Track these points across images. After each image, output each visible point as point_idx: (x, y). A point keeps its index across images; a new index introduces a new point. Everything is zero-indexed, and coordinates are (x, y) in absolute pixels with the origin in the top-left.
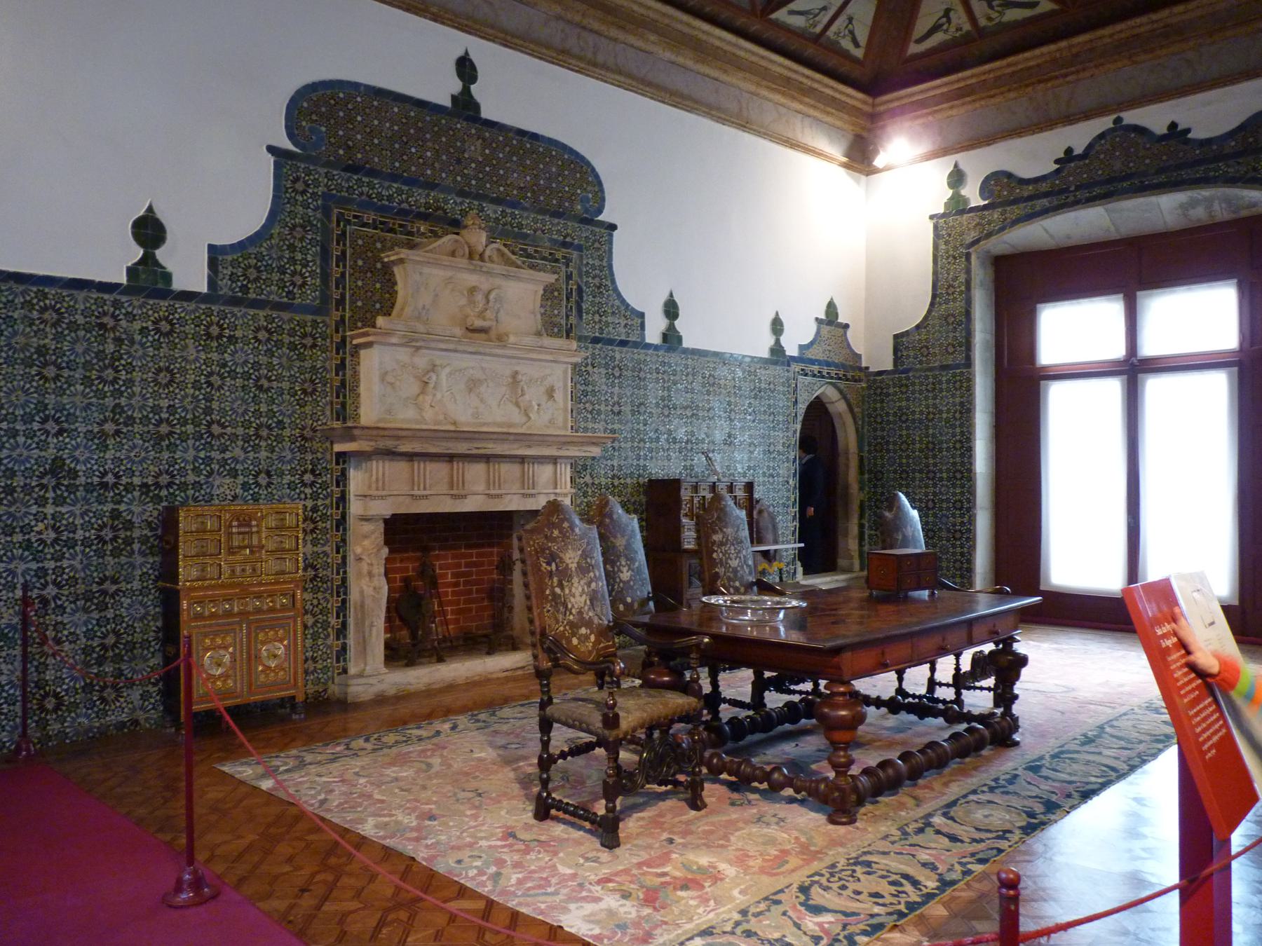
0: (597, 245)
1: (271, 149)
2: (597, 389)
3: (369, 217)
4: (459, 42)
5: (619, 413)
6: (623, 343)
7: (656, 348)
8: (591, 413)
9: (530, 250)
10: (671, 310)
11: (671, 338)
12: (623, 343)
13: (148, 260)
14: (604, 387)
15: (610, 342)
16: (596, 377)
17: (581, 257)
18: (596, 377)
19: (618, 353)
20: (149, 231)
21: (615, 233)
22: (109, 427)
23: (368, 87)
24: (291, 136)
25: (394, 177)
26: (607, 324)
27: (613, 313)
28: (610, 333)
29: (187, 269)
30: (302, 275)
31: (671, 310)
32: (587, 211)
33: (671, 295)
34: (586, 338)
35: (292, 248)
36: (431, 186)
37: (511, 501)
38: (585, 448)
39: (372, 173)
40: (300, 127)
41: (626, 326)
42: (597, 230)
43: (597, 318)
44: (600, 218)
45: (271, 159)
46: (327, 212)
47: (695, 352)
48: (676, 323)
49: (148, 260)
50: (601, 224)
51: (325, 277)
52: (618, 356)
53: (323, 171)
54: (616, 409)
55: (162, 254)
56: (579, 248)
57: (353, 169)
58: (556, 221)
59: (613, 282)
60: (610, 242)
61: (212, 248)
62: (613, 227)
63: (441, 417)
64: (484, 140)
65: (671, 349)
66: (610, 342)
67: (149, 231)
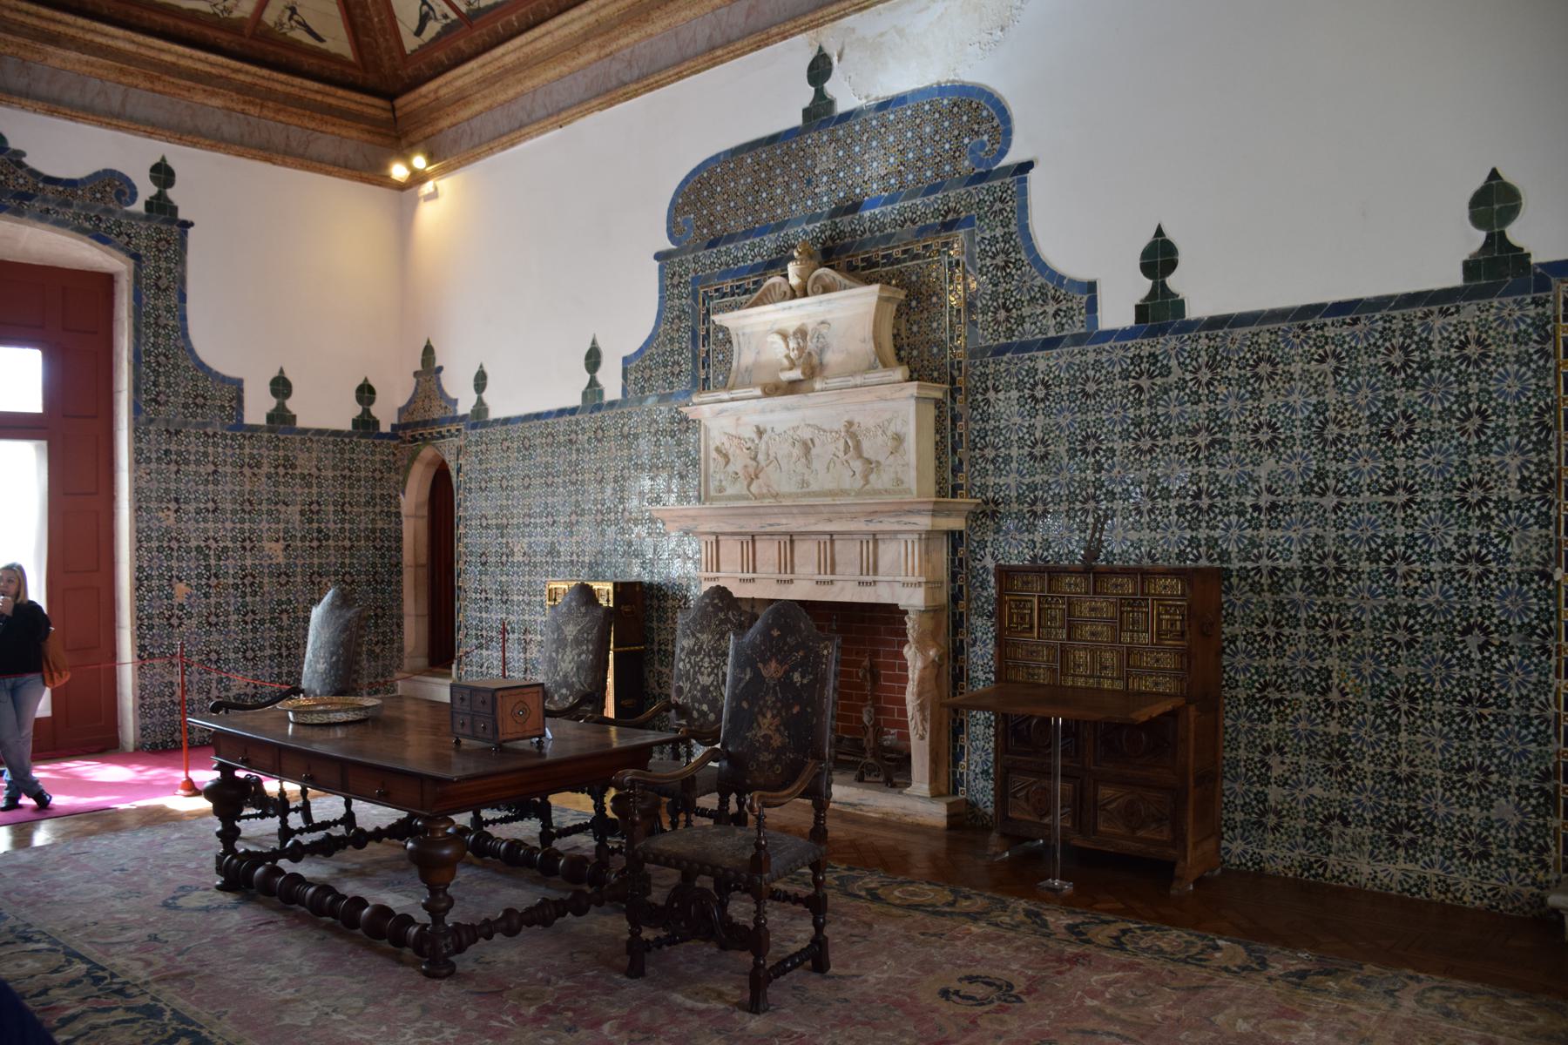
0: (998, 206)
1: (658, 256)
2: (1003, 424)
3: (727, 285)
4: (796, 52)
5: (1045, 457)
6: (1050, 344)
7: (1124, 334)
8: (993, 461)
9: (896, 253)
10: (1160, 258)
11: (1160, 311)
12: (1050, 344)
13: (593, 383)
14: (1018, 420)
15: (1024, 347)
16: (1001, 406)
17: (972, 235)
18: (1001, 406)
19: (1043, 362)
20: (593, 359)
21: (1032, 175)
22: (574, 518)
23: (725, 153)
24: (671, 236)
25: (747, 234)
26: (1021, 320)
27: (1032, 299)
28: (1030, 331)
29: (612, 384)
30: (678, 364)
31: (1160, 258)
32: (980, 162)
33: (1159, 232)
34: (984, 351)
35: (672, 340)
36: (780, 226)
37: (843, 589)
38: (905, 519)
39: (731, 238)
40: (676, 224)
41: (1056, 314)
42: (997, 183)
43: (1002, 315)
44: (1005, 162)
45: (657, 264)
46: (695, 294)
47: (1216, 323)
48: (1172, 281)
49: (593, 383)
50: (1006, 171)
51: (695, 357)
52: (1041, 365)
53: (690, 257)
54: (1039, 450)
55: (599, 375)
56: (969, 222)
57: (712, 244)
58: (932, 198)
59: (1031, 249)
60: (1023, 192)
61: (626, 360)
62: (1026, 166)
63: (765, 491)
64: (838, 140)
65: (1159, 330)
66: (1024, 347)
67: (593, 359)
